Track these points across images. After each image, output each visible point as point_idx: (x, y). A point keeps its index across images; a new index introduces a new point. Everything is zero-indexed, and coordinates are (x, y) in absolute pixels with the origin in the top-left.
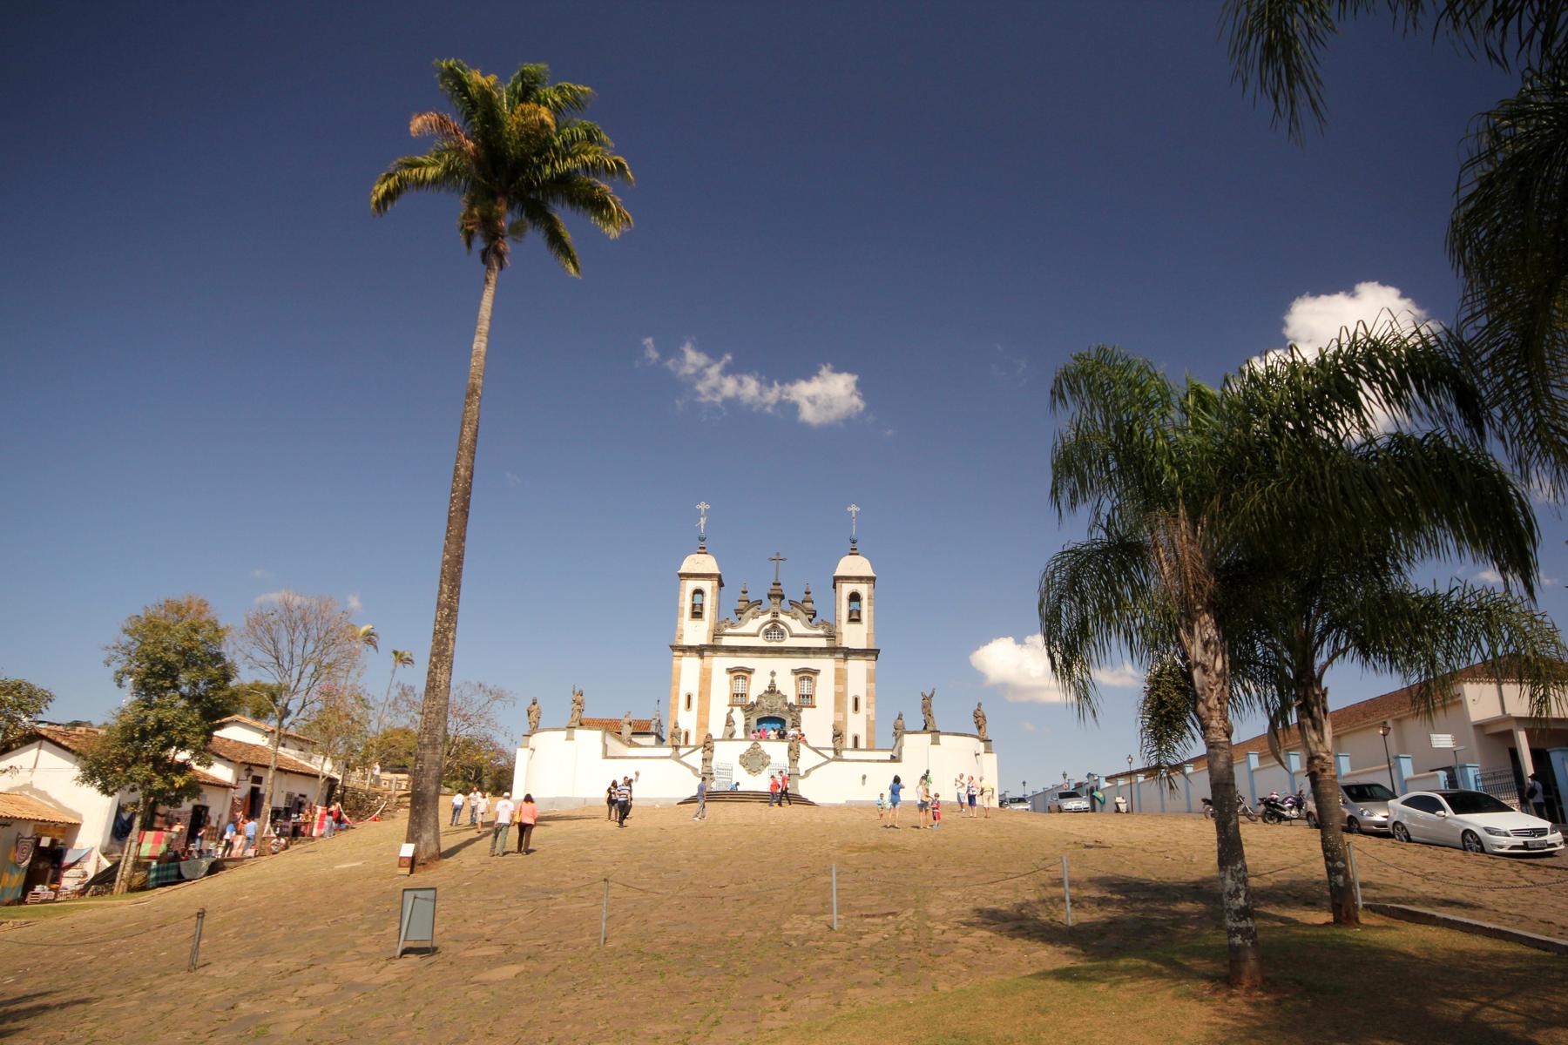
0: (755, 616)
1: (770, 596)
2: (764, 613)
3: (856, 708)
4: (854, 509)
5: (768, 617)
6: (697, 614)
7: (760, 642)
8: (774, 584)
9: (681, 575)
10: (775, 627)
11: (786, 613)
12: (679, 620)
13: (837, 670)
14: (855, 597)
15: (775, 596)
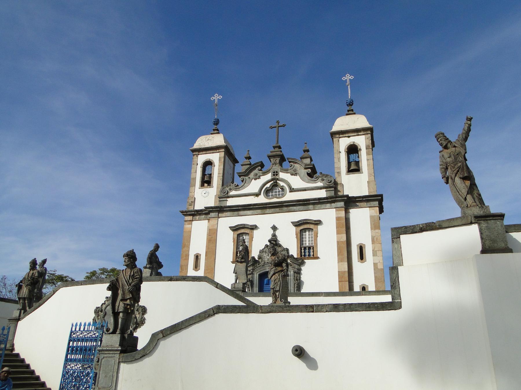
0: (257, 177)
1: (270, 157)
2: (265, 173)
3: (362, 257)
4: (348, 77)
5: (269, 177)
6: (206, 181)
7: (262, 199)
8: (274, 147)
9: (194, 151)
10: (275, 185)
11: (286, 171)
12: (191, 189)
13: (338, 219)
14: (353, 150)
15: (274, 156)
